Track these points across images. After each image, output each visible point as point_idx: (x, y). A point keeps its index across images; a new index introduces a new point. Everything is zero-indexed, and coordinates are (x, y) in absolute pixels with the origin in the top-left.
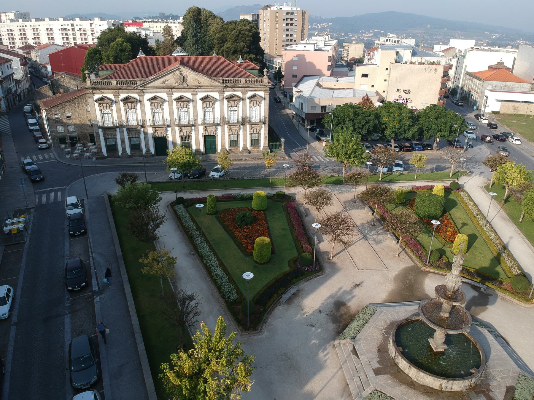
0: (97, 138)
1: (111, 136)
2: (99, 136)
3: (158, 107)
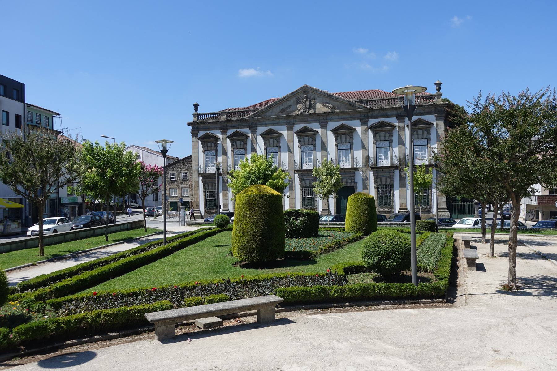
0: (196, 189)
1: (212, 186)
2: (199, 187)
3: (273, 144)
